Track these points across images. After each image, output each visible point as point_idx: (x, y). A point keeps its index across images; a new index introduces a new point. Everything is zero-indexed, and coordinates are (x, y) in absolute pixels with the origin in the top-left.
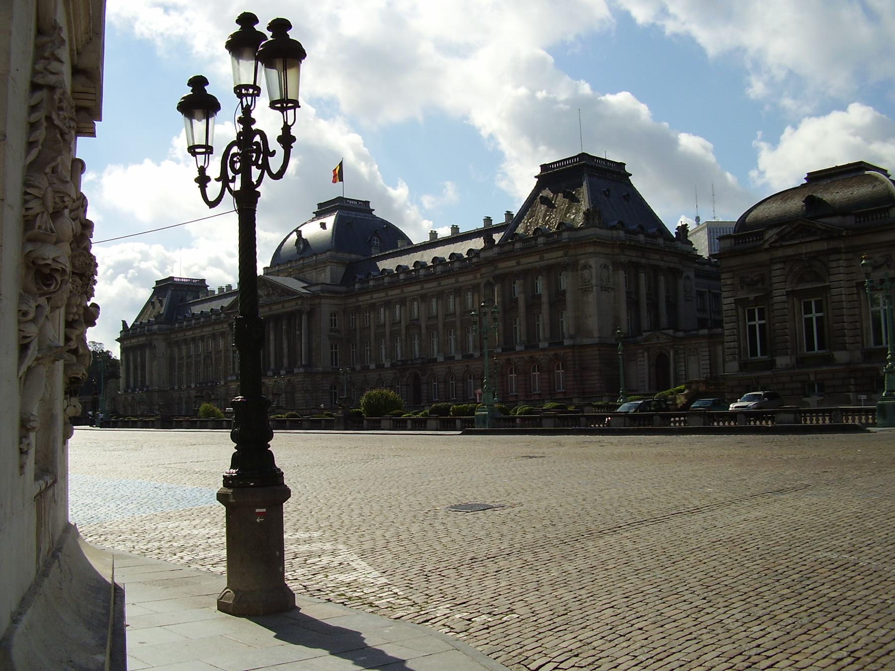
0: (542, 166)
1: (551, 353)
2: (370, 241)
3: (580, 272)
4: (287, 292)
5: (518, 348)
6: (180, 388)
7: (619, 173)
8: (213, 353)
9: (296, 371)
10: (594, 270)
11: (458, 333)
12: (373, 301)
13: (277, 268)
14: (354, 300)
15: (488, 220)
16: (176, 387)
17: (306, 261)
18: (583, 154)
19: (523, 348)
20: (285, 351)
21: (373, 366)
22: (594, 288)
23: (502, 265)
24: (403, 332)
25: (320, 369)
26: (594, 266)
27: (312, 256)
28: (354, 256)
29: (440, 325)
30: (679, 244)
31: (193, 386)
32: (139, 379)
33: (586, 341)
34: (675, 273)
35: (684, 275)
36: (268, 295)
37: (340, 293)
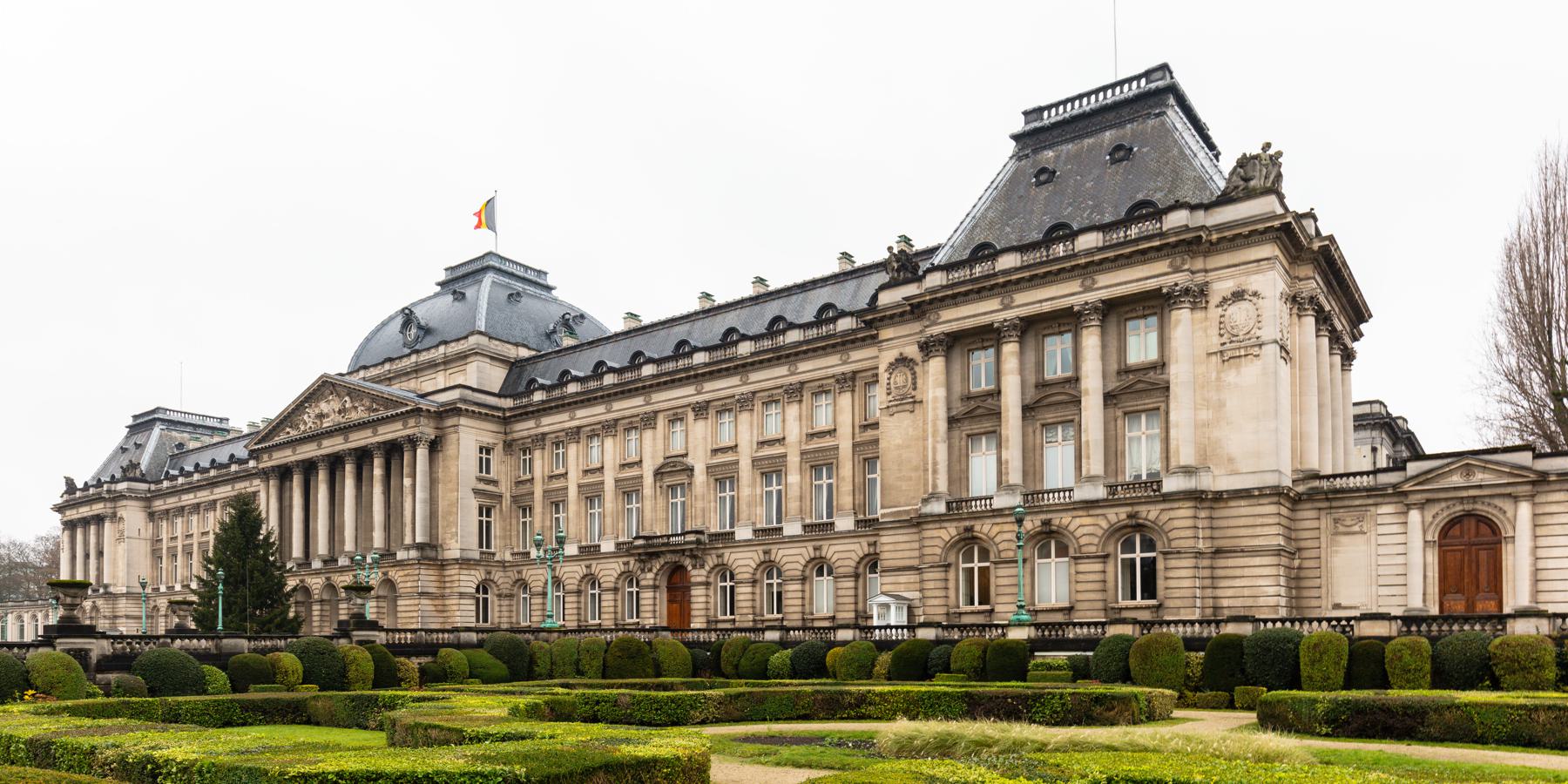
14: (531, 423)
17: (424, 357)
24: (648, 480)
28: (524, 353)
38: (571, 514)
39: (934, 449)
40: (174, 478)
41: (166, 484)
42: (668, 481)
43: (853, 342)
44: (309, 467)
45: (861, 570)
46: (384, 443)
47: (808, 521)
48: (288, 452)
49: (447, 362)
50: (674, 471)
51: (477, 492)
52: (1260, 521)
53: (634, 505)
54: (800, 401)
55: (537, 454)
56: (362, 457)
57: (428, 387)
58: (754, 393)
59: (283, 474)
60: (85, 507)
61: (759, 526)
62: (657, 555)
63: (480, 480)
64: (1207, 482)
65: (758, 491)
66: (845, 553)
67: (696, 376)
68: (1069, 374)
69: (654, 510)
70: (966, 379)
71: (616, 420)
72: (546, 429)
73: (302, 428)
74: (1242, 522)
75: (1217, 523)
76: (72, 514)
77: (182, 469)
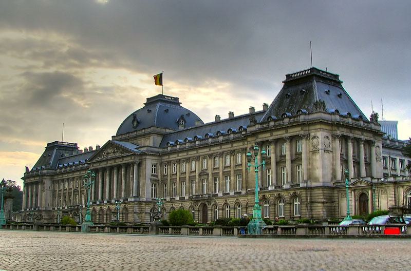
0: (286, 76)
1: (292, 192)
2: (178, 122)
3: (311, 141)
4: (125, 150)
5: (270, 188)
6: (59, 209)
7: (335, 81)
8: (79, 187)
9: (129, 200)
10: (320, 140)
12: (179, 158)
13: (120, 137)
14: (167, 157)
15: (252, 109)
16: (56, 209)
18: (314, 68)
20: (123, 187)
21: (177, 198)
22: (320, 151)
24: (197, 177)
25: (145, 199)
26: (320, 137)
27: (142, 130)
28: (168, 131)
29: (221, 173)
30: (373, 126)
31: (66, 208)
33: (314, 184)
34: (369, 143)
35: (376, 145)
36: (114, 152)
37: (158, 152)
42: (203, 177)
44: (104, 169)
46: (125, 163)
49: (144, 136)
50: (204, 173)
51: (151, 180)
52: (319, 195)
54: (234, 156)
55: (169, 167)
56: (119, 167)
59: (97, 171)
62: (199, 200)
63: (152, 175)
64: (309, 184)
74: (317, 195)
75: (313, 195)
76: (28, 181)
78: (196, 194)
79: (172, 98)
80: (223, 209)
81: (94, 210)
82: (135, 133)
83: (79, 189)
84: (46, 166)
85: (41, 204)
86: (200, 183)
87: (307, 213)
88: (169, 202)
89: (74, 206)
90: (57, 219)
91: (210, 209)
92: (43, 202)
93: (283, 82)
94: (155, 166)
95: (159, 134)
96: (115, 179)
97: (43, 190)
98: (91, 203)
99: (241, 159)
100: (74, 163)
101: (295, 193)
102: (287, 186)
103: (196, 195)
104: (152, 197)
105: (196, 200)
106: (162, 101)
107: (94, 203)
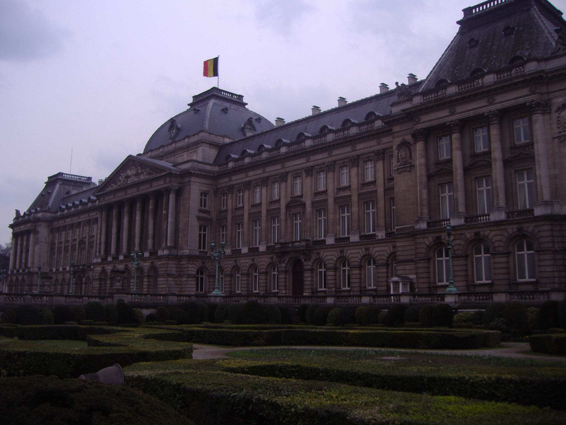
0: (464, 11)
1: (512, 229)
3: (555, 115)
9: (160, 253)
11: (355, 209)
12: (248, 179)
14: (227, 180)
19: (462, 221)
21: (245, 250)
23: (424, 118)
24: (283, 211)
25: (186, 252)
27: (184, 139)
28: (227, 141)
29: (331, 201)
31: (68, 269)
32: (23, 261)
36: (137, 174)
37: (211, 172)
38: (245, 230)
39: (421, 192)
40: (63, 210)
41: (59, 213)
42: (293, 211)
43: (383, 132)
44: (120, 205)
45: (390, 261)
47: (363, 234)
48: (112, 197)
49: (187, 148)
50: (296, 204)
51: (199, 218)
53: (276, 225)
55: (230, 196)
56: (145, 199)
57: (180, 160)
58: (335, 162)
59: (109, 208)
60: (23, 226)
61: (338, 236)
62: (287, 253)
63: (200, 211)
65: (338, 217)
66: (381, 251)
67: (306, 153)
68: (487, 150)
69: (286, 226)
70: (436, 153)
71: (268, 178)
72: (234, 183)
73: (119, 184)
76: (18, 229)
77: (67, 206)
78: (282, 241)
79: (232, 94)
80: (335, 269)
81: (104, 271)
82: (173, 145)
83: (87, 240)
84: (41, 207)
85: (33, 263)
86: (289, 222)
87: (556, 274)
88: (229, 257)
89: (79, 266)
90: (69, 284)
91: (308, 267)
92: (36, 261)
93: (458, 23)
94: (205, 196)
95: (213, 145)
96: (138, 218)
97: (36, 243)
98: (99, 260)
99: (372, 172)
100: (81, 201)
101: (520, 230)
102: (498, 216)
103: (282, 244)
104: (200, 248)
105: (280, 251)
106: (217, 97)
107: (104, 260)
